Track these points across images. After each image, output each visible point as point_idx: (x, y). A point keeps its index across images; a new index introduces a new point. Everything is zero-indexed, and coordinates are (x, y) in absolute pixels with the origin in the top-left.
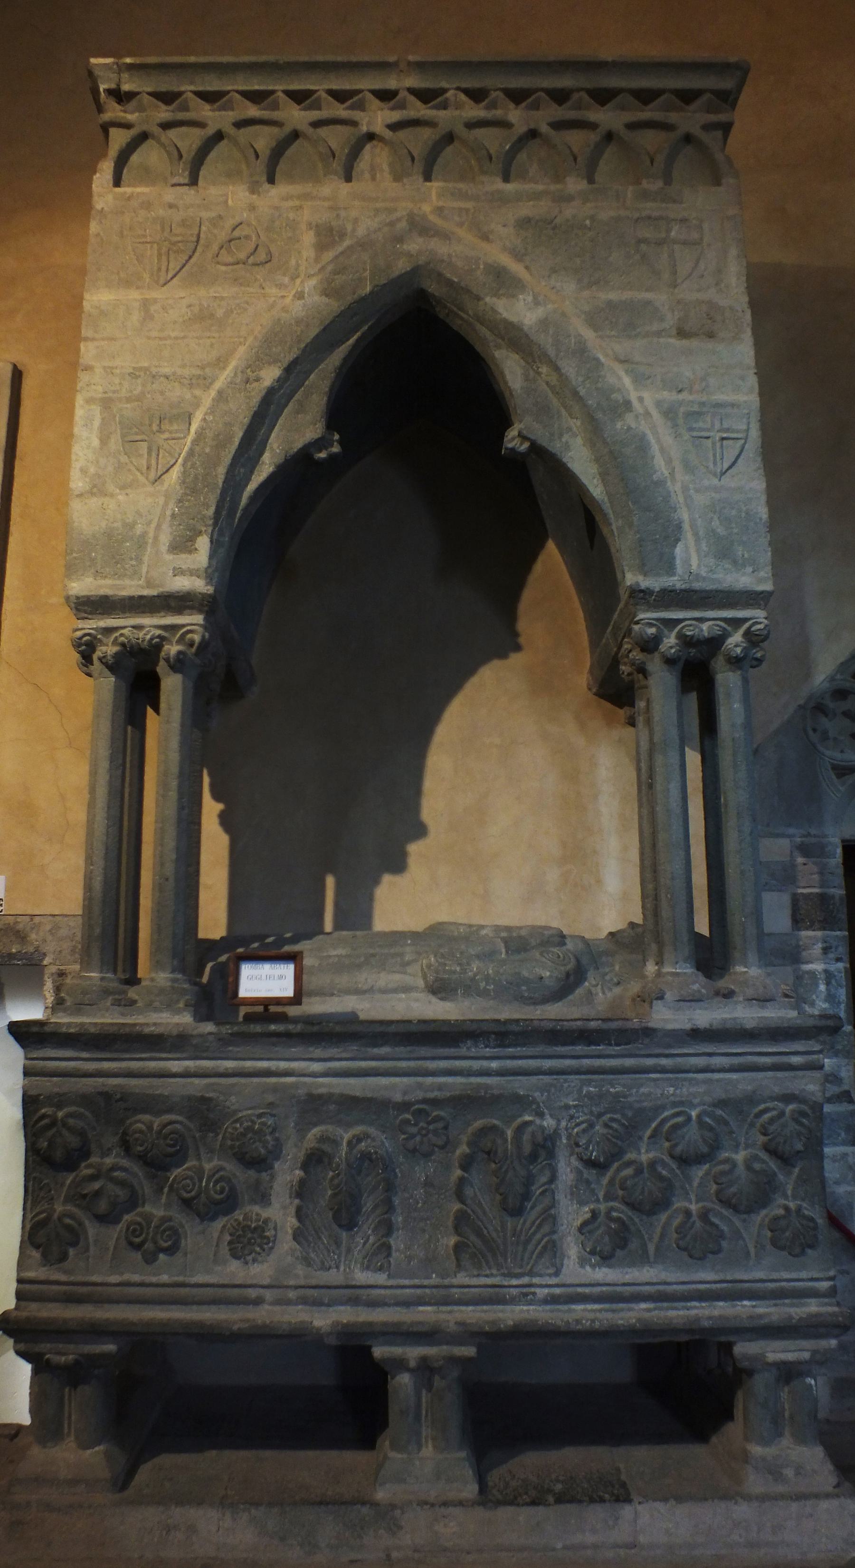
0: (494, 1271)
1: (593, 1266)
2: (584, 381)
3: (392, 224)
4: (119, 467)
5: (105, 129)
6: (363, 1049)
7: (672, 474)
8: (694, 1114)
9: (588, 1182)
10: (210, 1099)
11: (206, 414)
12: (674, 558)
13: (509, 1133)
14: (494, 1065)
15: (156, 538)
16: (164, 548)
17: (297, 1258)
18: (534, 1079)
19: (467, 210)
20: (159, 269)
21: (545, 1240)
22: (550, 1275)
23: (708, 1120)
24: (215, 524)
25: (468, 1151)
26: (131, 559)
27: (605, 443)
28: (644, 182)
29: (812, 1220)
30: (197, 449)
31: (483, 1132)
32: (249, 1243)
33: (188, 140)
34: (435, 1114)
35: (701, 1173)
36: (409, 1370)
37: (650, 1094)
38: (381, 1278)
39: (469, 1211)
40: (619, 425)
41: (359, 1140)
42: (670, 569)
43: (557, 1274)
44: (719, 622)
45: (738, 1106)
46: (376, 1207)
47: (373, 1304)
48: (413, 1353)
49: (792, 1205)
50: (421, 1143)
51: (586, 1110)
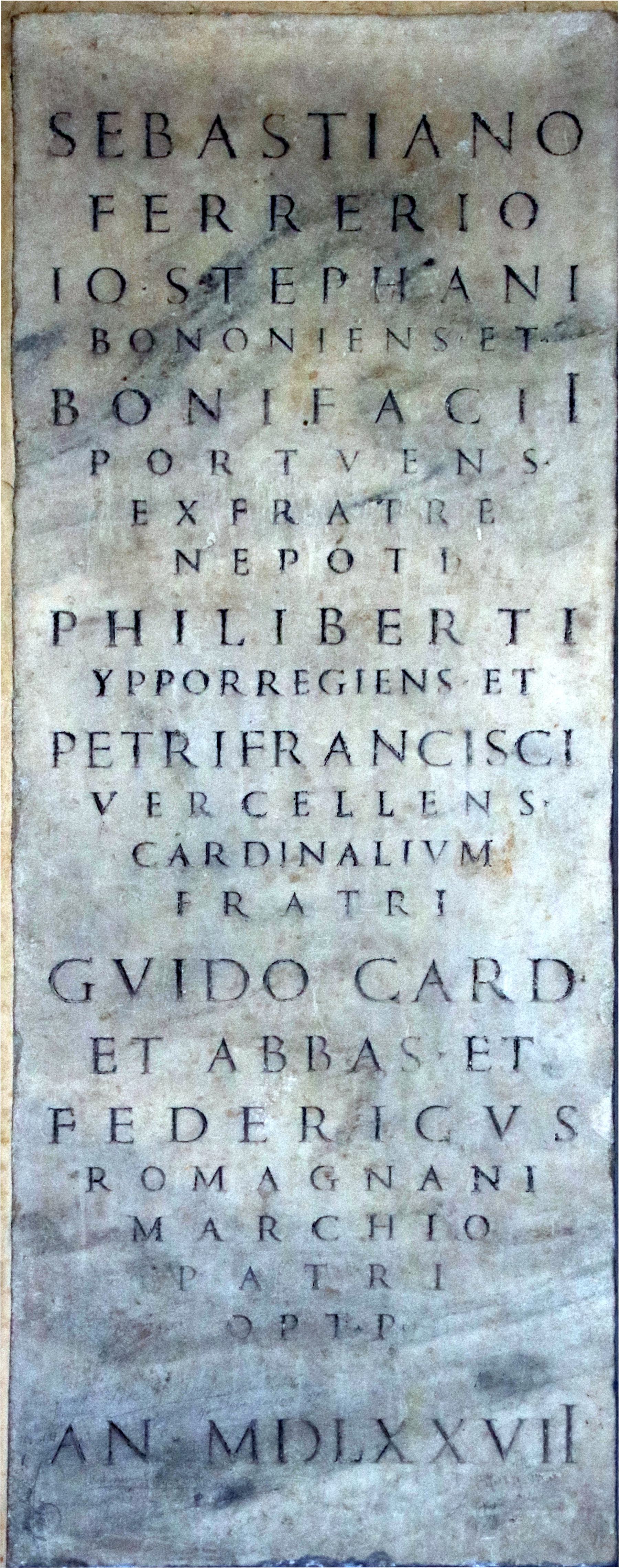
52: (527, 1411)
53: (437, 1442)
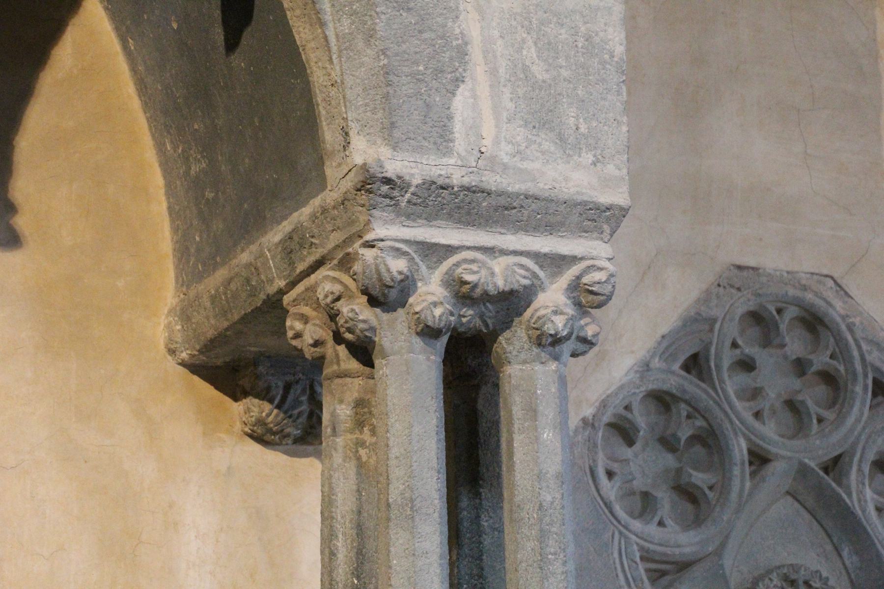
12: (450, 118)
42: (443, 140)
44: (524, 261)
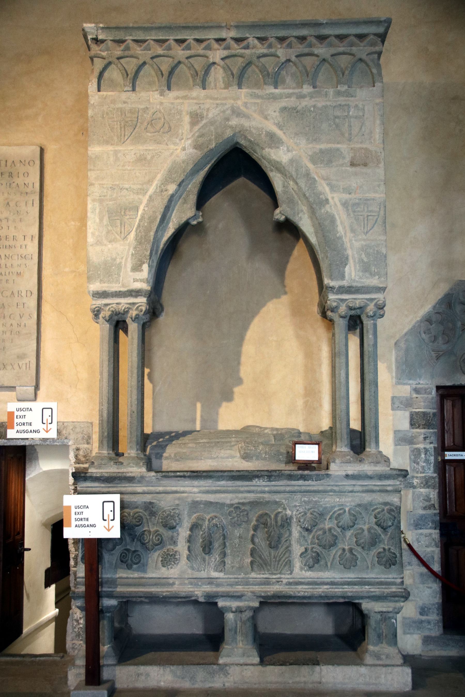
0: (266, 572)
1: (306, 571)
2: (308, 189)
3: (224, 112)
4: (108, 232)
5: (92, 59)
6: (214, 482)
7: (345, 234)
8: (347, 509)
9: (304, 537)
10: (153, 503)
11: (145, 207)
12: (345, 272)
13: (273, 516)
14: (267, 489)
15: (125, 265)
16: (129, 269)
17: (188, 567)
18: (282, 495)
19: (258, 103)
20: (121, 135)
21: (287, 560)
22: (288, 574)
23: (353, 512)
24: (150, 258)
25: (256, 523)
26: (115, 274)
27: (316, 218)
28: (339, 86)
29: (394, 554)
30: (142, 224)
31: (261, 516)
32: (169, 561)
33: (131, 65)
34: (243, 508)
35: (350, 534)
36: (232, 612)
37: (329, 501)
38: (221, 575)
39: (256, 548)
40: (323, 211)
41: (213, 519)
42: (342, 277)
43: (291, 574)
45: (366, 507)
46: (219, 546)
47: (218, 585)
48: (234, 604)
49: (386, 547)
50: (238, 520)
51: (303, 508)
52: (24, 362)
53: (11, 367)
